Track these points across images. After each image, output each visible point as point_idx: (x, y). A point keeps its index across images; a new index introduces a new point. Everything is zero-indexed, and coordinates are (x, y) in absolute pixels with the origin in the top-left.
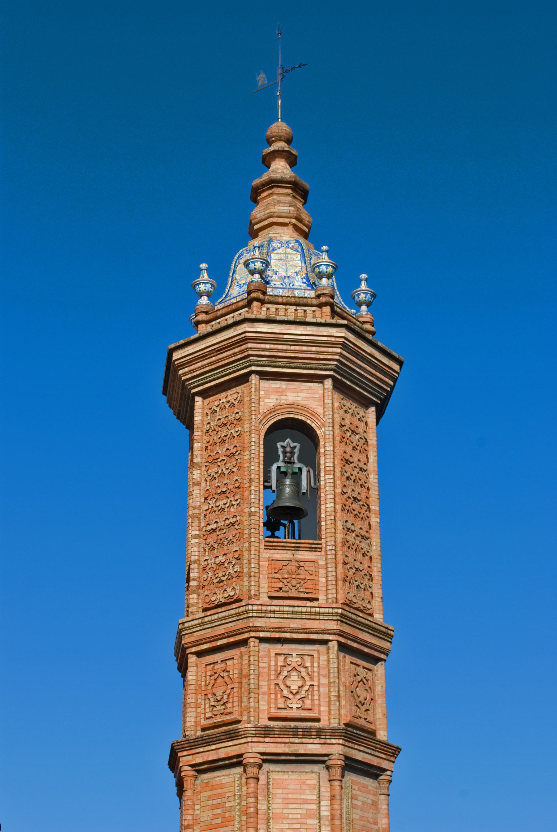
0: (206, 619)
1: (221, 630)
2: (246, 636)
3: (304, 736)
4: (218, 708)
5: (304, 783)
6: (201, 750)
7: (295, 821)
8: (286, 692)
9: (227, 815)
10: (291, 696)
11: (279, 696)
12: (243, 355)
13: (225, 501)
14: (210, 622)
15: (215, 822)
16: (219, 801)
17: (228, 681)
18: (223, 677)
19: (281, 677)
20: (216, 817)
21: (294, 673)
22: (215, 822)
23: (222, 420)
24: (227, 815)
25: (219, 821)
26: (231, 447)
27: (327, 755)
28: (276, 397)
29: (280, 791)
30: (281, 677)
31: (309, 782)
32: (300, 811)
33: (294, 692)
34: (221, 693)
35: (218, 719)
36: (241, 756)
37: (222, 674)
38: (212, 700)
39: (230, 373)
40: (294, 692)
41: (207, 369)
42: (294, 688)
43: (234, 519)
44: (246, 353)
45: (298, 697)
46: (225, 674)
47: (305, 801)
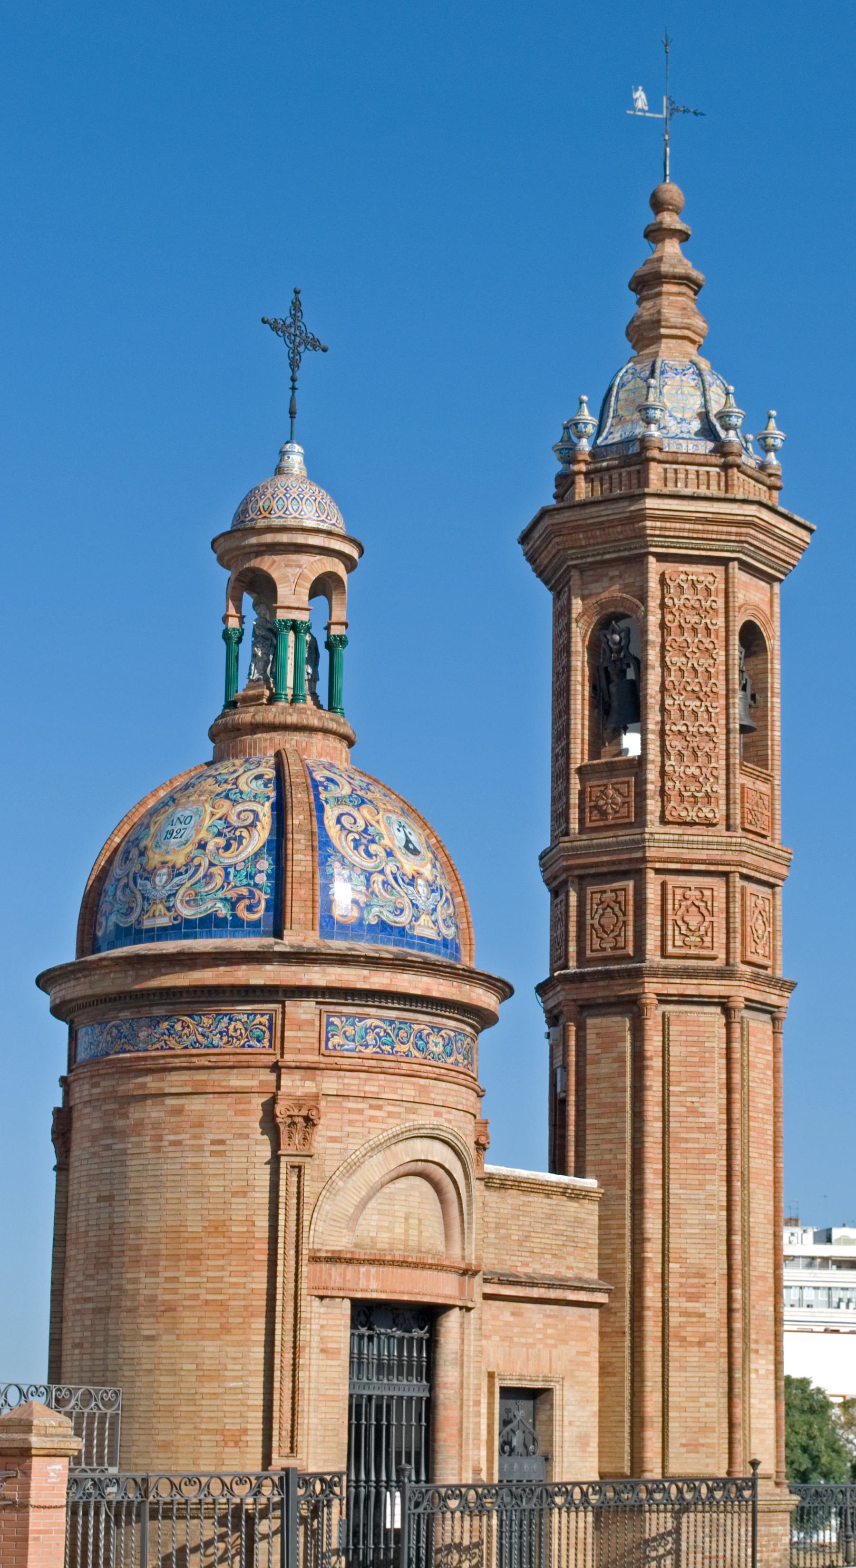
0: (686, 838)
1: (702, 855)
2: (733, 869)
3: (768, 985)
6: (678, 981)
9: (707, 1055)
12: (738, 538)
14: (688, 842)
15: (689, 1059)
18: (698, 907)
20: (692, 1054)
22: (689, 1059)
24: (707, 1055)
25: (697, 1059)
27: (778, 1007)
34: (695, 923)
35: (693, 951)
36: (728, 997)
37: (697, 903)
41: (686, 534)
44: (743, 538)
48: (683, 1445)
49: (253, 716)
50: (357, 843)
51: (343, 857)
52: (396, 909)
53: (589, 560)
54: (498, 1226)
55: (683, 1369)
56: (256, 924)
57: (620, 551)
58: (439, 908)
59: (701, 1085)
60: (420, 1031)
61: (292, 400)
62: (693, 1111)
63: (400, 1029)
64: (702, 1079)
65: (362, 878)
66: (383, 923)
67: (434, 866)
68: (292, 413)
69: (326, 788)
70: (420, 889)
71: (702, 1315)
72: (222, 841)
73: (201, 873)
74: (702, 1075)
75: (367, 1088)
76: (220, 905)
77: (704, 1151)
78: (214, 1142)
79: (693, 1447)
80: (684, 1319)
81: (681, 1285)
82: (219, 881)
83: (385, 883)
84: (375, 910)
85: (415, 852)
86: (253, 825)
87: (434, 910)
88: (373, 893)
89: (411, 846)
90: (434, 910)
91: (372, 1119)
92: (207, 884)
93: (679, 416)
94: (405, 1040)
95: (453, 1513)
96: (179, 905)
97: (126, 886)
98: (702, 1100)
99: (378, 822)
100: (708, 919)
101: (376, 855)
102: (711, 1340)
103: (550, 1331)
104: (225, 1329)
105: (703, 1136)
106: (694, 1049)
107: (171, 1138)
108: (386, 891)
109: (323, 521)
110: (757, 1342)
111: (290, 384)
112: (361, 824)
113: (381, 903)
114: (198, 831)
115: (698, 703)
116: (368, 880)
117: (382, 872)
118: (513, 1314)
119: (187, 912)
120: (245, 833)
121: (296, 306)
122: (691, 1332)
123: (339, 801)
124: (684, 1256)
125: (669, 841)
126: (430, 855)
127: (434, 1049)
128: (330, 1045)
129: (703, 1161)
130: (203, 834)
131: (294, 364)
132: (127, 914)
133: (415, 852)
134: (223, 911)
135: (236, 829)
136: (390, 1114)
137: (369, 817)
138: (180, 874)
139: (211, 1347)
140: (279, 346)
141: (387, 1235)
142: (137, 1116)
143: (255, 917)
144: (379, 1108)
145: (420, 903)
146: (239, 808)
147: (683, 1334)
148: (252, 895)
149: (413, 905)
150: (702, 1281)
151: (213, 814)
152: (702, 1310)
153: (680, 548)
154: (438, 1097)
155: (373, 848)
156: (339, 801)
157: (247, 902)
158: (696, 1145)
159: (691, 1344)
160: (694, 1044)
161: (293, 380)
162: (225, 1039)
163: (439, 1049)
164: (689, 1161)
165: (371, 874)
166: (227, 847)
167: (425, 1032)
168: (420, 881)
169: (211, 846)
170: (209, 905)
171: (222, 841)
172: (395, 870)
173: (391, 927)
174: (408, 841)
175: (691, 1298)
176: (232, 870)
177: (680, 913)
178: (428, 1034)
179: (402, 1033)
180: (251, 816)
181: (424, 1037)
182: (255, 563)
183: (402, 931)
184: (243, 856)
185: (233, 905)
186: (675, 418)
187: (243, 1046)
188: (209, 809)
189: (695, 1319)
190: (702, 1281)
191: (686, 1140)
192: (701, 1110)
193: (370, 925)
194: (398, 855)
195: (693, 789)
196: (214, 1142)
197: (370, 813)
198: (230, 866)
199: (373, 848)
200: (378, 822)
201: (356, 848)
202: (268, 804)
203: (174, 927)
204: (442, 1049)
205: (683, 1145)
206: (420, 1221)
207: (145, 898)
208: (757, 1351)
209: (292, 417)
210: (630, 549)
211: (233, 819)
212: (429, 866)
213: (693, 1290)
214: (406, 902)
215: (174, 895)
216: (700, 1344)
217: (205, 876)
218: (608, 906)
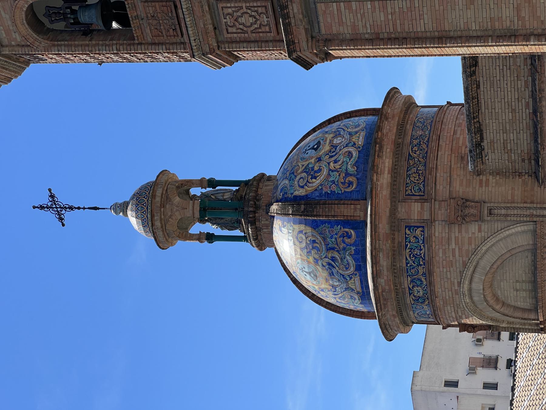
5: (325, 12)
7: (356, 18)
8: (256, 26)
10: (258, 22)
11: (260, 30)
19: (245, 29)
21: (240, 20)
28: (13, 34)
29: (334, 28)
30: (245, 29)
31: (324, 8)
32: (347, 14)
33: (254, 20)
39: (6, 61)
40: (254, 20)
42: (251, 20)
45: (258, 17)
47: (339, 10)
54: (505, 131)
58: (341, 271)
61: (89, 208)
68: (95, 208)
127: (421, 293)
131: (71, 208)
154: (447, 294)
161: (79, 208)
204: (419, 288)
206: (517, 281)
209: (98, 209)
212: (318, 267)
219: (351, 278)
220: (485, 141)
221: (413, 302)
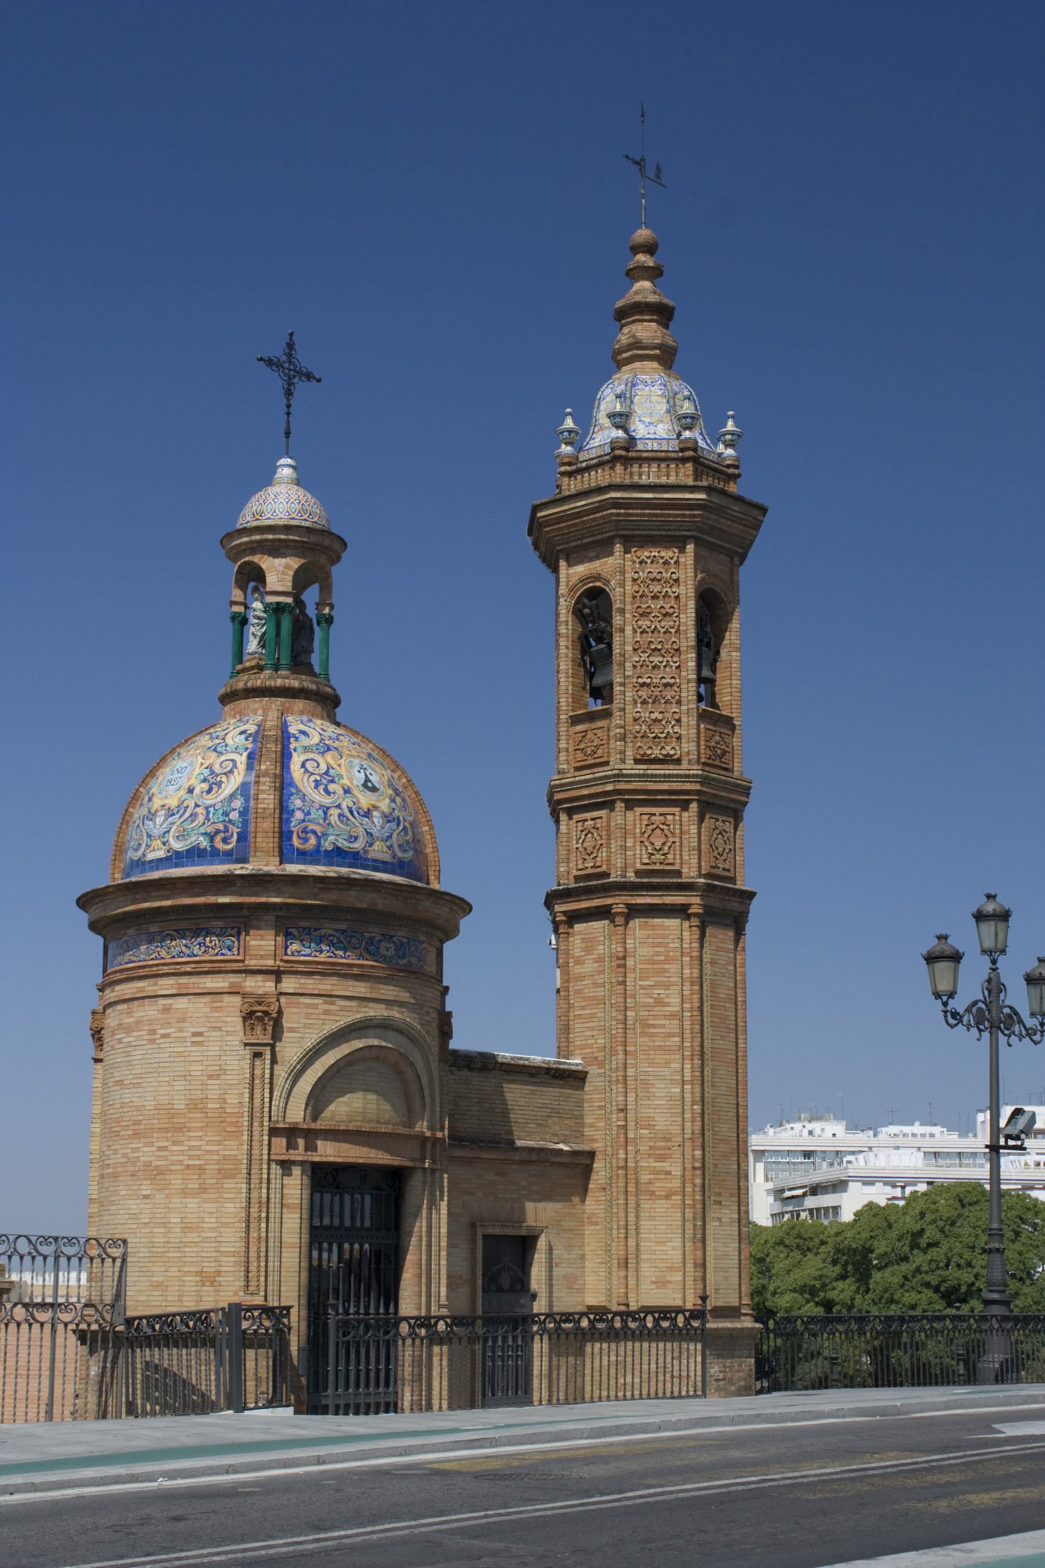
4: (658, 856)
9: (671, 954)
13: (661, 659)
14: (652, 776)
15: (655, 958)
16: (661, 940)
17: (669, 834)
18: (662, 830)
22: (655, 958)
23: (655, 574)
25: (662, 958)
26: (667, 606)
34: (660, 844)
35: (658, 867)
37: (661, 826)
38: (650, 848)
43: (673, 681)
46: (665, 827)
48: (652, 1282)
49: (245, 684)
50: (317, 784)
51: (304, 795)
52: (351, 837)
53: (572, 544)
55: (652, 1218)
56: (228, 854)
57: (594, 535)
58: (395, 835)
59: (666, 979)
60: (372, 938)
61: (288, 422)
62: (659, 1002)
63: (352, 936)
64: (667, 975)
65: (321, 812)
66: (338, 848)
67: (393, 801)
68: (288, 434)
69: (297, 739)
70: (375, 820)
71: (669, 1173)
72: (205, 786)
73: (188, 814)
74: (667, 971)
75: (321, 987)
76: (201, 838)
77: (670, 1035)
78: (194, 1034)
79: (661, 1283)
80: (653, 1177)
81: (651, 1148)
82: (201, 818)
83: (340, 815)
84: (331, 838)
85: (374, 789)
86: (231, 772)
87: (390, 837)
88: (329, 824)
89: (369, 784)
90: (390, 837)
91: (327, 1012)
92: (193, 821)
93: (647, 420)
94: (357, 946)
95: (404, 1340)
96: (171, 840)
97: (138, 826)
98: (668, 992)
99: (339, 765)
100: (671, 840)
101: (334, 793)
102: (675, 1193)
103: (534, 1188)
104: (202, 1189)
105: (668, 1022)
106: (660, 949)
107: (162, 1031)
108: (342, 822)
109: (305, 520)
110: (719, 1195)
111: (286, 410)
112: (323, 767)
113: (336, 832)
114: (189, 779)
115: (661, 659)
116: (325, 813)
117: (339, 806)
118: (497, 1174)
119: (178, 846)
120: (224, 779)
121: (291, 346)
122: (661, 1186)
123: (306, 749)
124: (652, 1123)
125: (635, 776)
126: (390, 792)
127: (386, 953)
128: (289, 951)
129: (668, 1044)
130: (193, 781)
131: (289, 393)
132: (137, 850)
133: (374, 789)
134: (204, 843)
135: (217, 775)
136: (343, 1009)
137: (331, 762)
138: (173, 814)
139: (192, 1204)
140: (275, 380)
141: (345, 1109)
142: (139, 1014)
143: (230, 847)
144: (333, 1004)
145: (375, 831)
146: (223, 758)
147: (652, 1189)
148: (226, 830)
149: (367, 833)
150: (669, 1144)
151: (202, 764)
152: (668, 1169)
153: (644, 530)
155: (332, 787)
156: (306, 749)
157: (222, 835)
158: (662, 1030)
159: (659, 1197)
160: (659, 945)
161: (288, 406)
162: (203, 949)
163: (392, 952)
164: (657, 1044)
165: (328, 808)
166: (209, 791)
167: (377, 939)
168: (375, 813)
169: (197, 791)
170: (194, 839)
171: (205, 786)
172: (351, 804)
173: (346, 852)
174: (367, 780)
175: (661, 1158)
176: (211, 809)
177: (646, 835)
178: (380, 941)
179: (354, 941)
180: (231, 764)
181: (375, 943)
182: (256, 559)
183: (356, 855)
184: (221, 797)
185: (212, 837)
186: (644, 422)
187: (217, 954)
188: (200, 760)
189: (662, 1177)
190: (669, 1144)
191: (654, 1026)
192: (666, 1000)
193: (326, 851)
194: (356, 792)
195: (657, 731)
196: (194, 1034)
197: (334, 758)
198: (211, 806)
199: (332, 787)
200: (339, 765)
201: (316, 787)
202: (245, 754)
203: (167, 858)
204: (393, 953)
205: (651, 1030)
207: (149, 836)
208: (719, 1203)
209: (287, 437)
210: (602, 533)
211: (217, 769)
212: (387, 801)
213: (661, 1152)
214: (361, 831)
215: (168, 832)
216: (667, 1197)
217: (191, 815)
218: (589, 832)
219: (389, 848)
220: (469, 1074)
221: (367, 935)
